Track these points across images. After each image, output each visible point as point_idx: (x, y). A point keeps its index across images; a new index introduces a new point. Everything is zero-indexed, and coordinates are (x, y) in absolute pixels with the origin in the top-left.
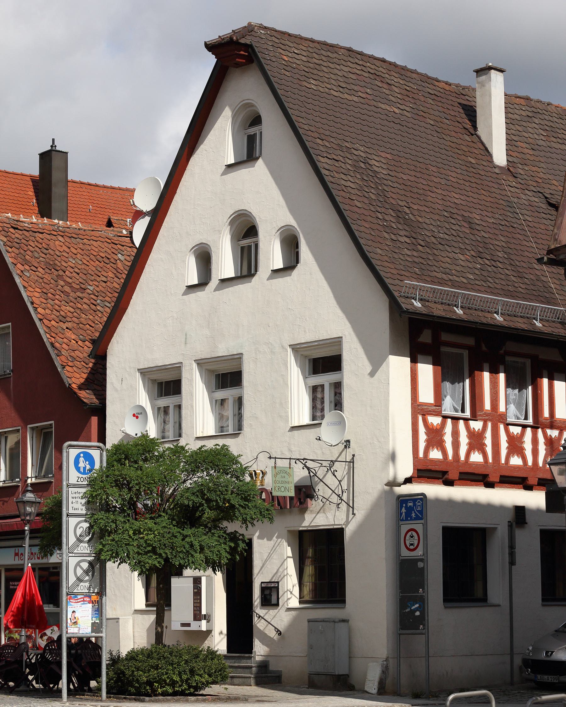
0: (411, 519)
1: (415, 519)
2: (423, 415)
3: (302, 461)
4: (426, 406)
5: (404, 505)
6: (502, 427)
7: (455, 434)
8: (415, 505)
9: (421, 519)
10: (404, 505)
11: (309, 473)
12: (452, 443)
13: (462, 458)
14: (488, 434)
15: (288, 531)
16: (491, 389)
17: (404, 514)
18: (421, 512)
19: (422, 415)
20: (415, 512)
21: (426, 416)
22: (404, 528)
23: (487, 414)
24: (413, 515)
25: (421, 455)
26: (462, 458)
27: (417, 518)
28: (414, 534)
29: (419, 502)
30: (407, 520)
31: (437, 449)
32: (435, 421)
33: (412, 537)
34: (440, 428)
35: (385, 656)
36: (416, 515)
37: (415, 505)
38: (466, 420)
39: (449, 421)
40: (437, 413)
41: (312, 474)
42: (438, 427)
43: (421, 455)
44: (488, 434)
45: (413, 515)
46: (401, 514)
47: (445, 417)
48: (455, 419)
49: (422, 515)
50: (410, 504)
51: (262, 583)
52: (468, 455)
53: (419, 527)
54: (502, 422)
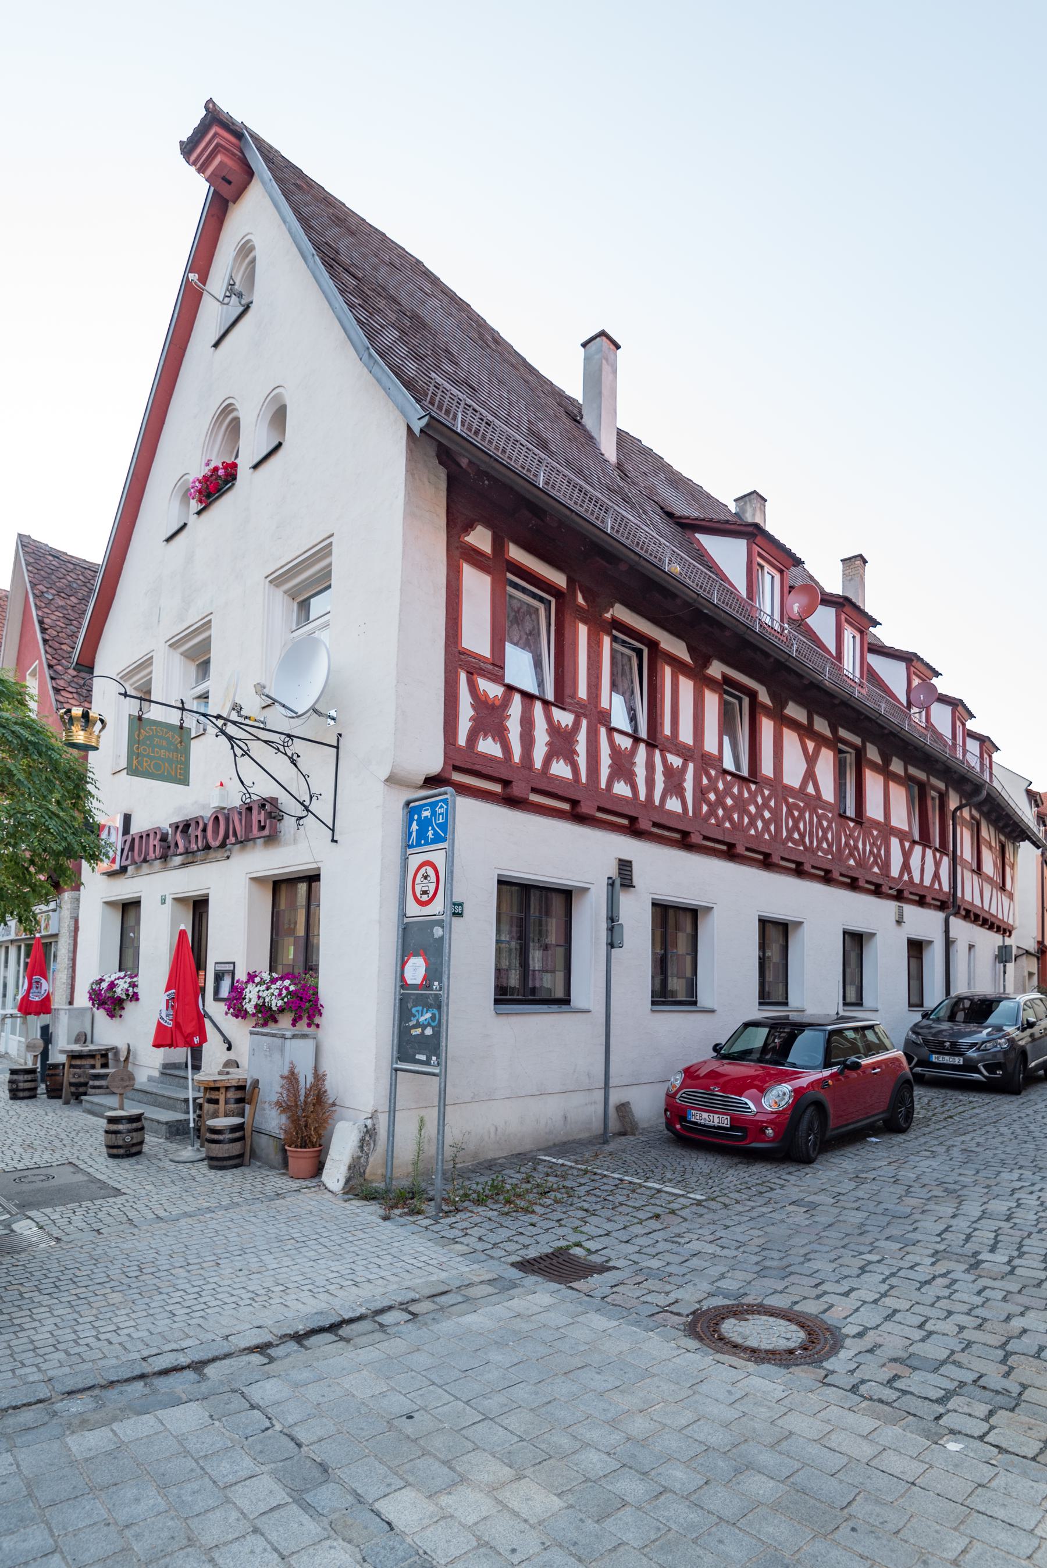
0: (427, 843)
1: (434, 841)
2: (469, 673)
3: (214, 720)
4: (474, 658)
5: (416, 817)
6: (603, 731)
7: (527, 723)
8: (434, 813)
9: (444, 840)
10: (416, 817)
11: (232, 747)
12: (521, 736)
13: (538, 764)
14: (582, 737)
15: (251, 879)
16: (588, 669)
17: (414, 834)
18: (443, 826)
19: (468, 672)
20: (433, 829)
21: (475, 676)
22: (415, 861)
23: (580, 704)
24: (430, 834)
25: (462, 741)
26: (538, 764)
27: (438, 839)
28: (431, 871)
29: (441, 807)
30: (419, 845)
31: (494, 739)
32: (493, 690)
33: (426, 877)
34: (501, 706)
35: (370, 1109)
36: (435, 833)
37: (434, 813)
38: (546, 703)
39: (517, 698)
40: (497, 677)
41: (239, 752)
42: (497, 703)
43: (462, 741)
44: (582, 737)
45: (430, 834)
46: (410, 834)
47: (510, 688)
48: (527, 696)
49: (445, 833)
50: (426, 814)
51: (216, 963)
52: (547, 762)
53: (438, 858)
54: (604, 725)
